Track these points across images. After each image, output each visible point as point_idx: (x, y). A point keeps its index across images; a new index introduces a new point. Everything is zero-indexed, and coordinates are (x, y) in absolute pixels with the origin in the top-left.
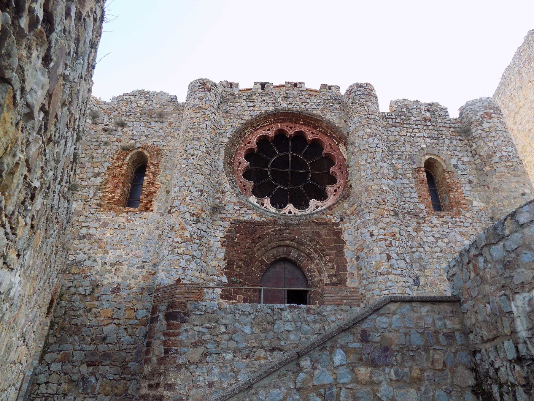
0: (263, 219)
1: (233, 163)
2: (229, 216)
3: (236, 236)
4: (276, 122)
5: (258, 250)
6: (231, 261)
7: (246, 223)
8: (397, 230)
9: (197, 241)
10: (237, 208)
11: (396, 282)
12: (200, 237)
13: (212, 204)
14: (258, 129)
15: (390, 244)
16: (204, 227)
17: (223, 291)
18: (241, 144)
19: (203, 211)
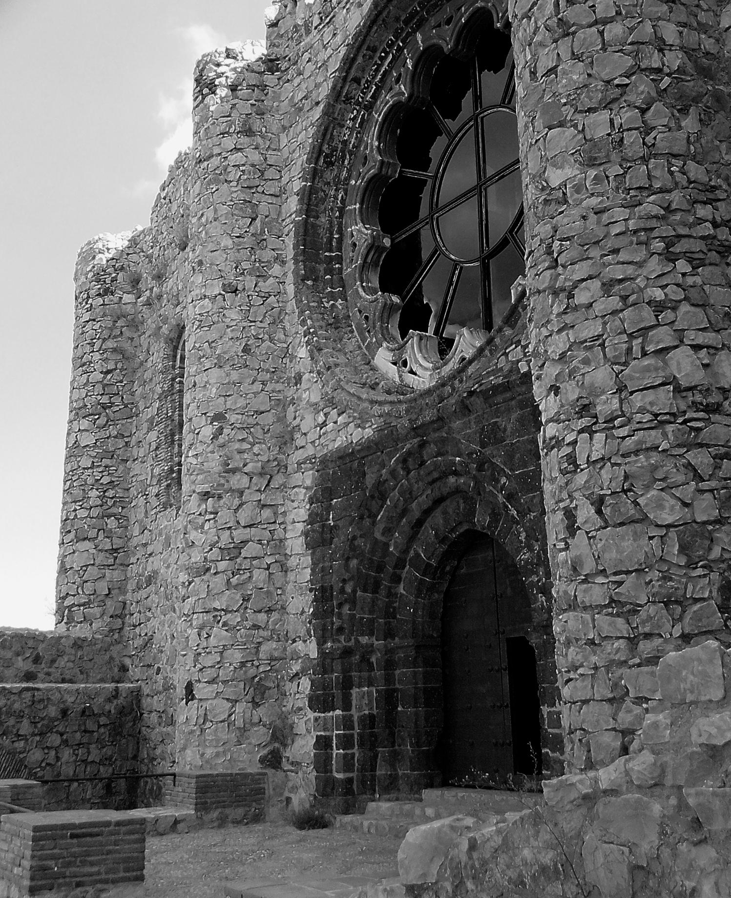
0: (369, 432)
1: (340, 259)
2: (310, 451)
3: (329, 508)
4: (409, 34)
5: (388, 531)
6: (323, 589)
7: (340, 458)
8: (601, 375)
9: (222, 565)
10: (321, 418)
11: (592, 642)
12: (234, 551)
13: (278, 428)
14: (375, 97)
15: (572, 459)
16: (244, 516)
17: (312, 681)
18: (348, 179)
19: (234, 471)
